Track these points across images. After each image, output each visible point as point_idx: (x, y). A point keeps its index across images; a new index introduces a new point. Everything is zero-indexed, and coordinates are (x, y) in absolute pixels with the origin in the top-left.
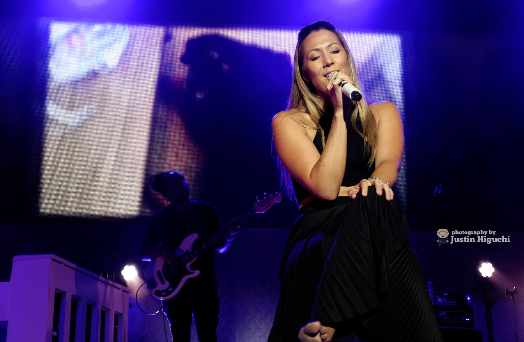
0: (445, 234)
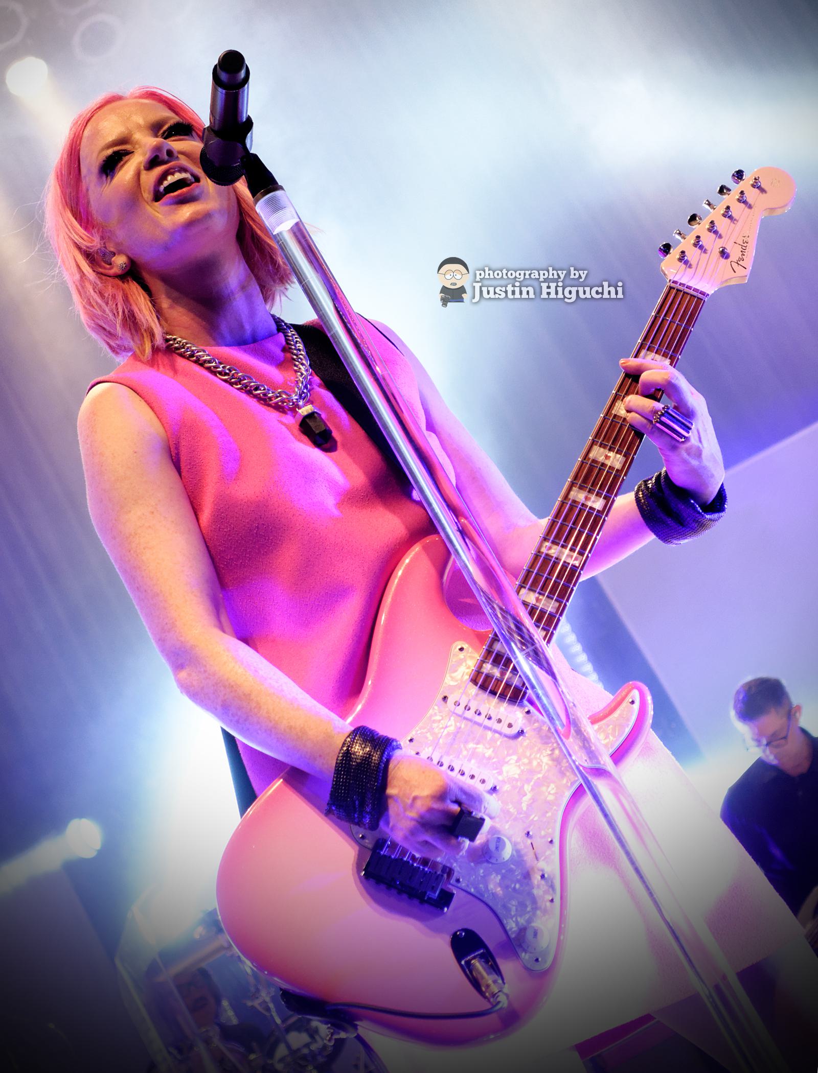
0: (459, 276)
